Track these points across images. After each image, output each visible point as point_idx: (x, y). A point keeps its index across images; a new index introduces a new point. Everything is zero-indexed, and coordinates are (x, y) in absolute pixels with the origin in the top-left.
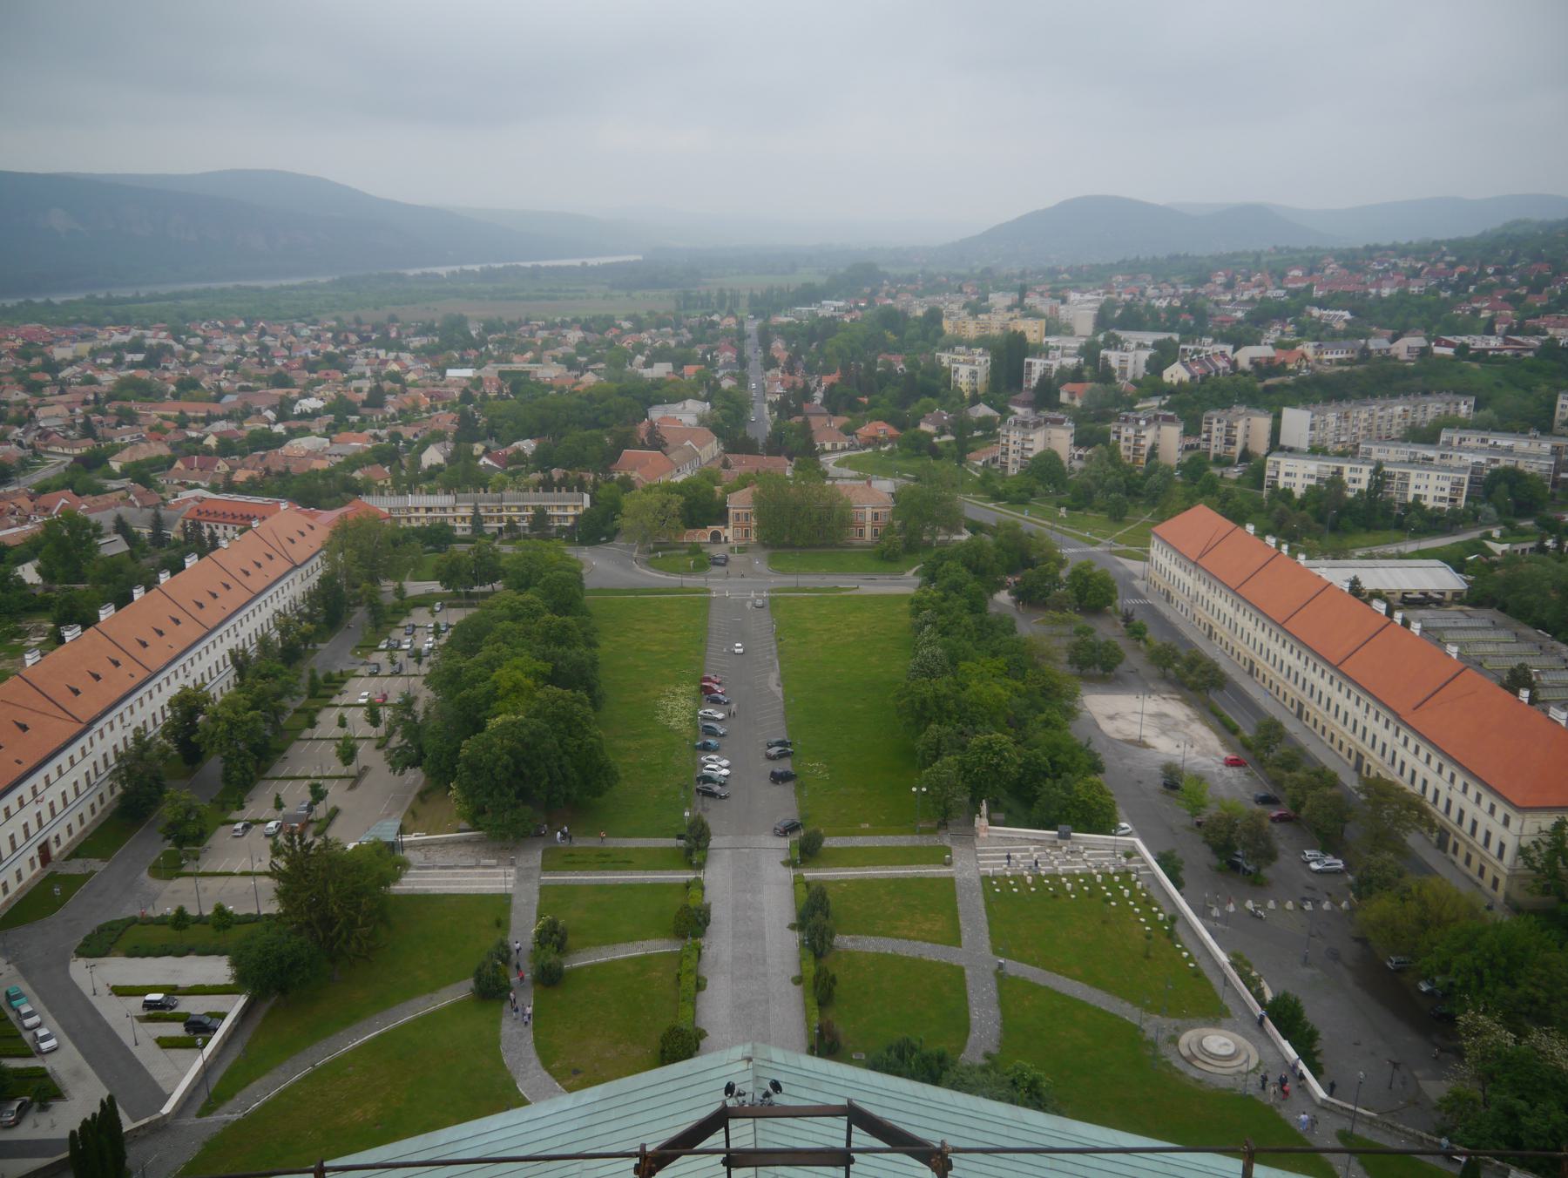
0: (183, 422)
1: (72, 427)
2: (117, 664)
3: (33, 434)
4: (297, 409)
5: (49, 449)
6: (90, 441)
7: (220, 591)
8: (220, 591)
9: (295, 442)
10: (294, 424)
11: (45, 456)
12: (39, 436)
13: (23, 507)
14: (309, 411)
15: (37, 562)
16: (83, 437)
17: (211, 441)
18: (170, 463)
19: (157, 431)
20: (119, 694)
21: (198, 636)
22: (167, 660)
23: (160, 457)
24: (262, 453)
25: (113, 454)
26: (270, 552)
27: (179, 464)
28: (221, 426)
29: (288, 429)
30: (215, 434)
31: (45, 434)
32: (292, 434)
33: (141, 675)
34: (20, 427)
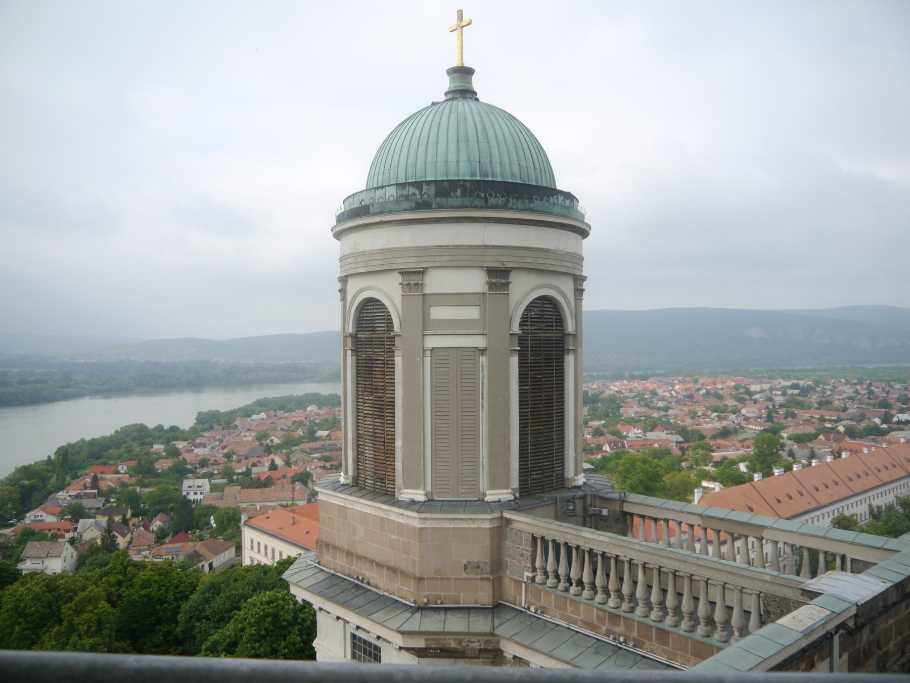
0: (822, 420)
1: (760, 418)
2: (801, 494)
3: (740, 418)
4: (895, 419)
5: (748, 426)
6: (770, 424)
7: (863, 475)
8: (863, 475)
9: (893, 433)
10: (894, 426)
11: (746, 429)
12: (744, 419)
13: (737, 445)
14: (903, 420)
15: (746, 463)
16: (767, 421)
17: (841, 429)
18: (816, 436)
19: (809, 422)
20: (802, 510)
21: (847, 495)
22: (830, 501)
23: (810, 434)
24: (873, 437)
25: (783, 430)
26: (893, 462)
27: (821, 437)
28: (844, 422)
29: (889, 427)
30: (843, 426)
31: (747, 419)
32: (891, 430)
33: (814, 505)
34: (734, 414)
